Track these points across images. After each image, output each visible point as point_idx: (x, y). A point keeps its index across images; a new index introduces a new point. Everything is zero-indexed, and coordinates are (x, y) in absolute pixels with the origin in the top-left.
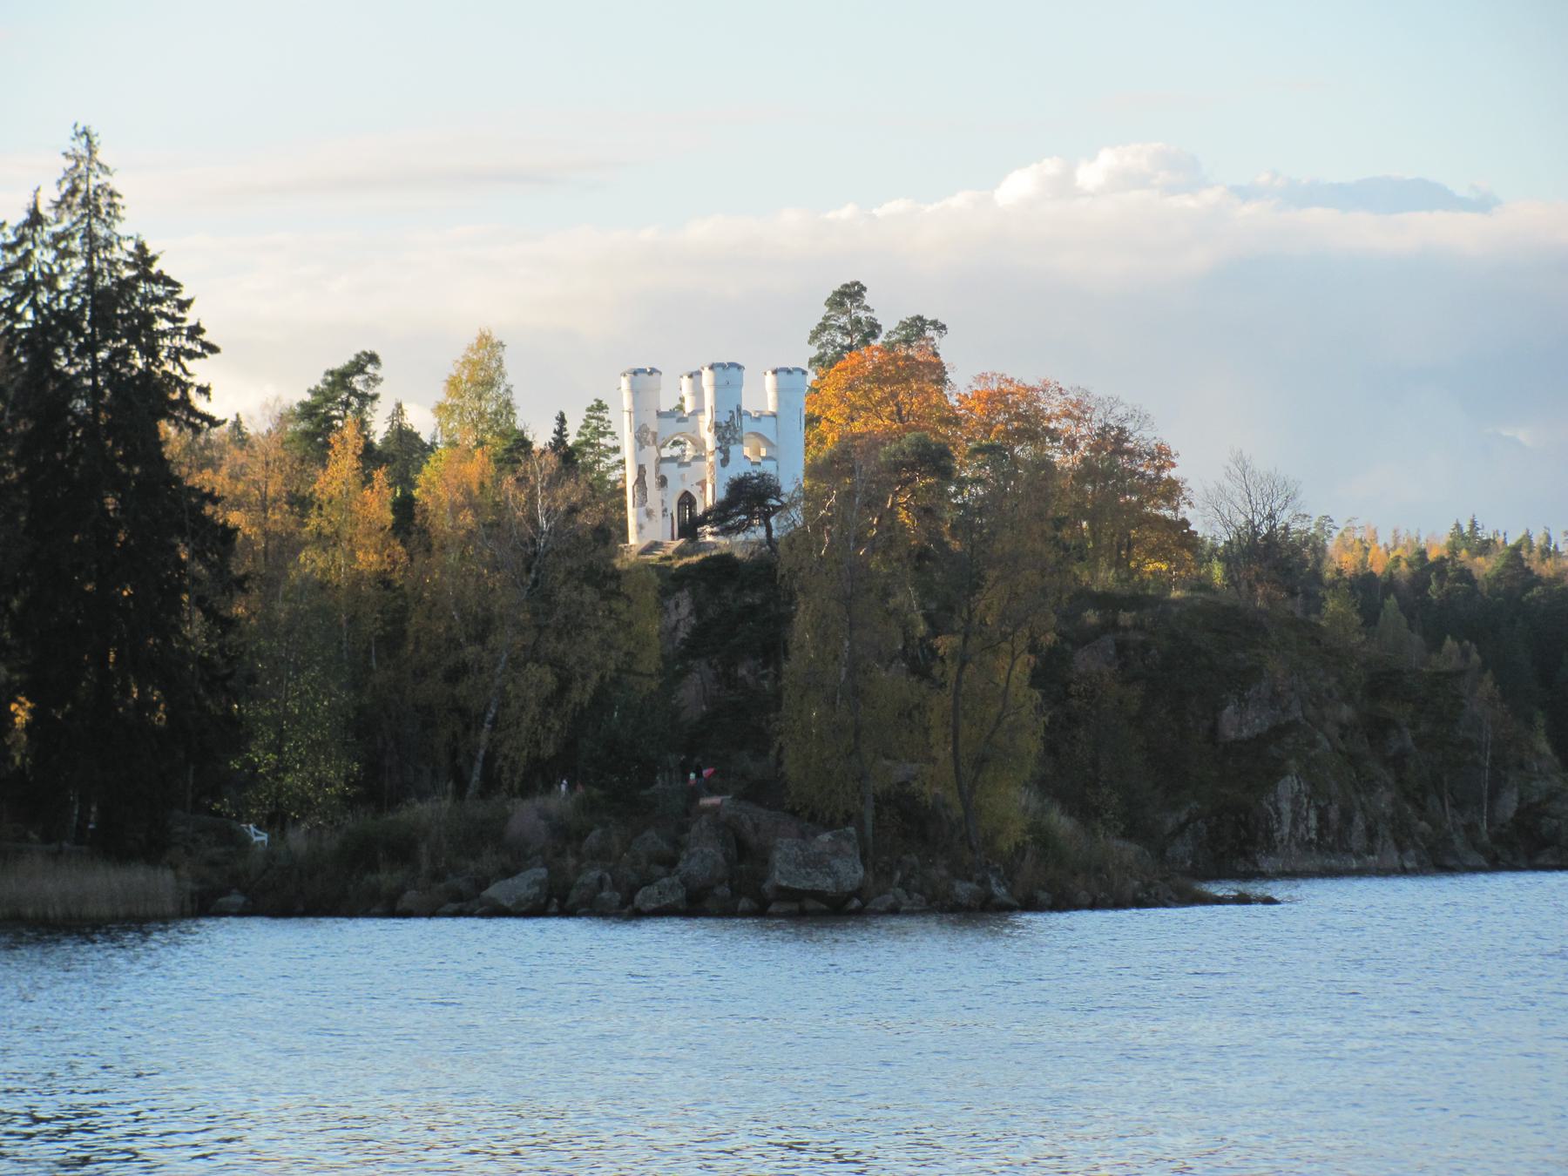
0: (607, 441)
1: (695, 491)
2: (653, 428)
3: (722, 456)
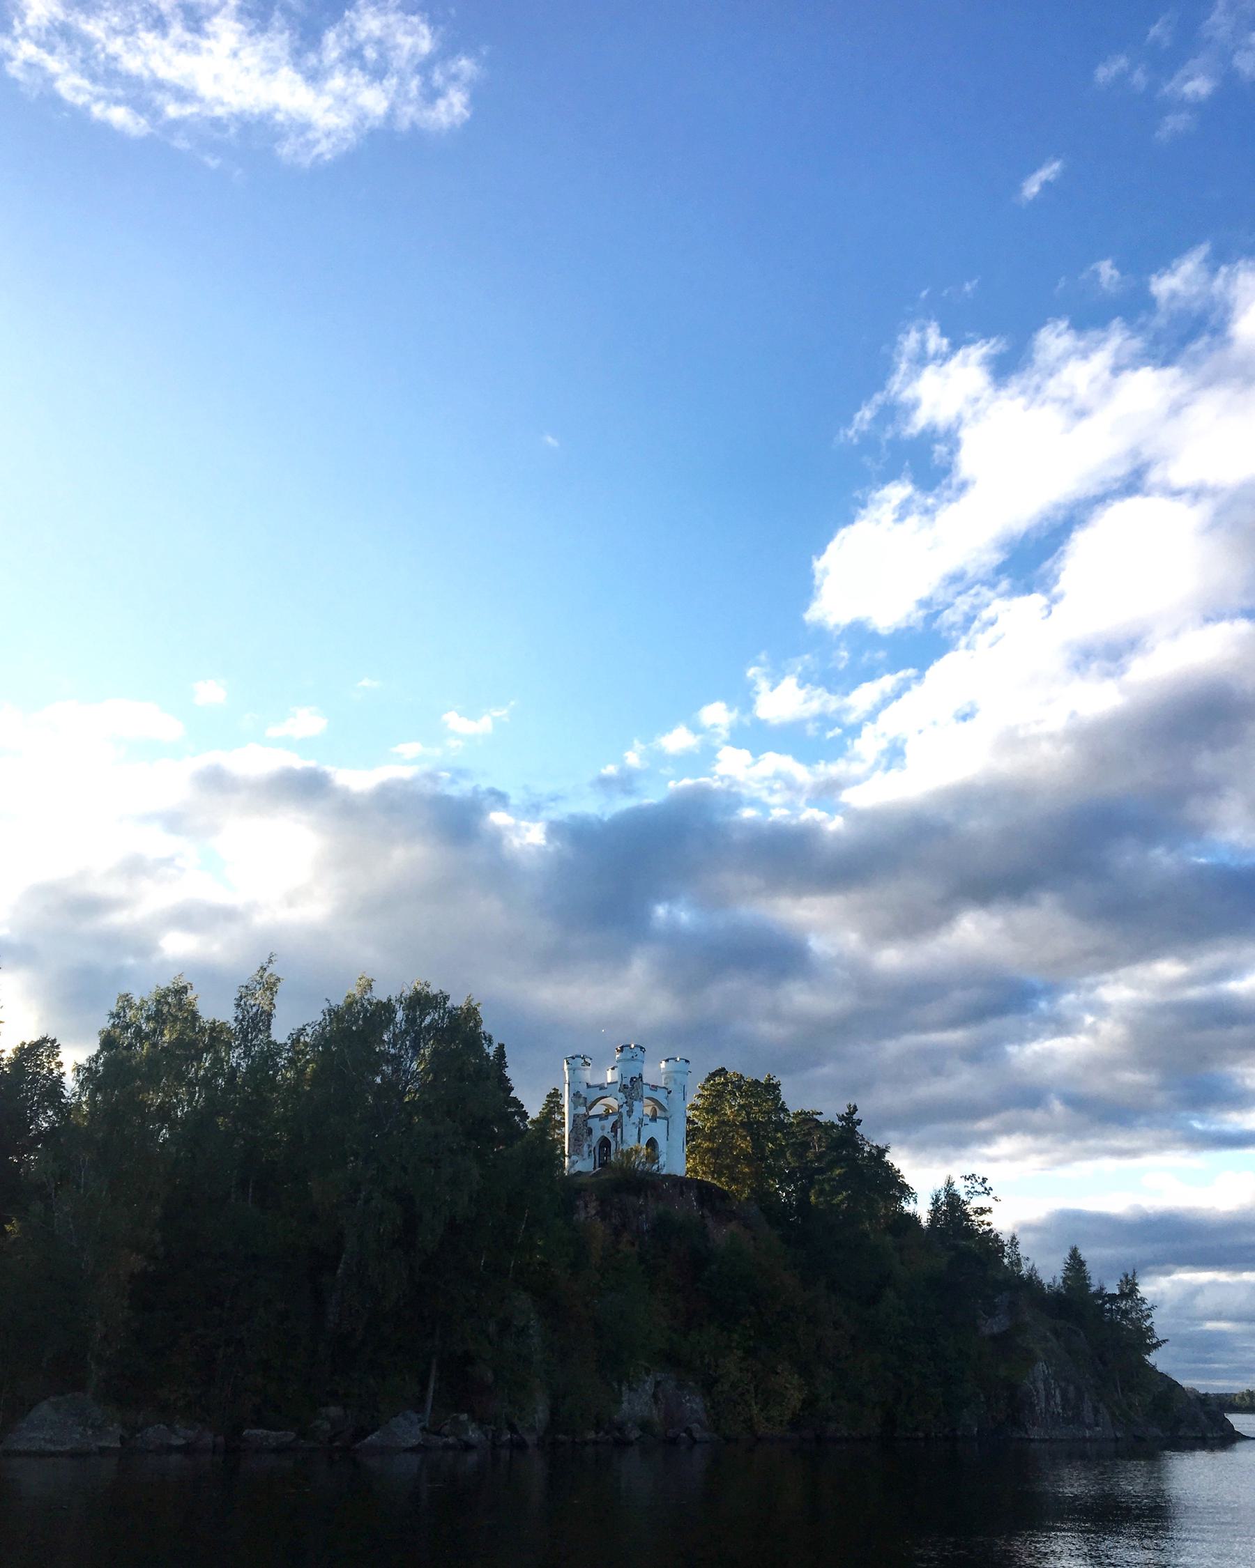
0: (558, 1117)
1: (610, 1136)
3: (628, 1108)
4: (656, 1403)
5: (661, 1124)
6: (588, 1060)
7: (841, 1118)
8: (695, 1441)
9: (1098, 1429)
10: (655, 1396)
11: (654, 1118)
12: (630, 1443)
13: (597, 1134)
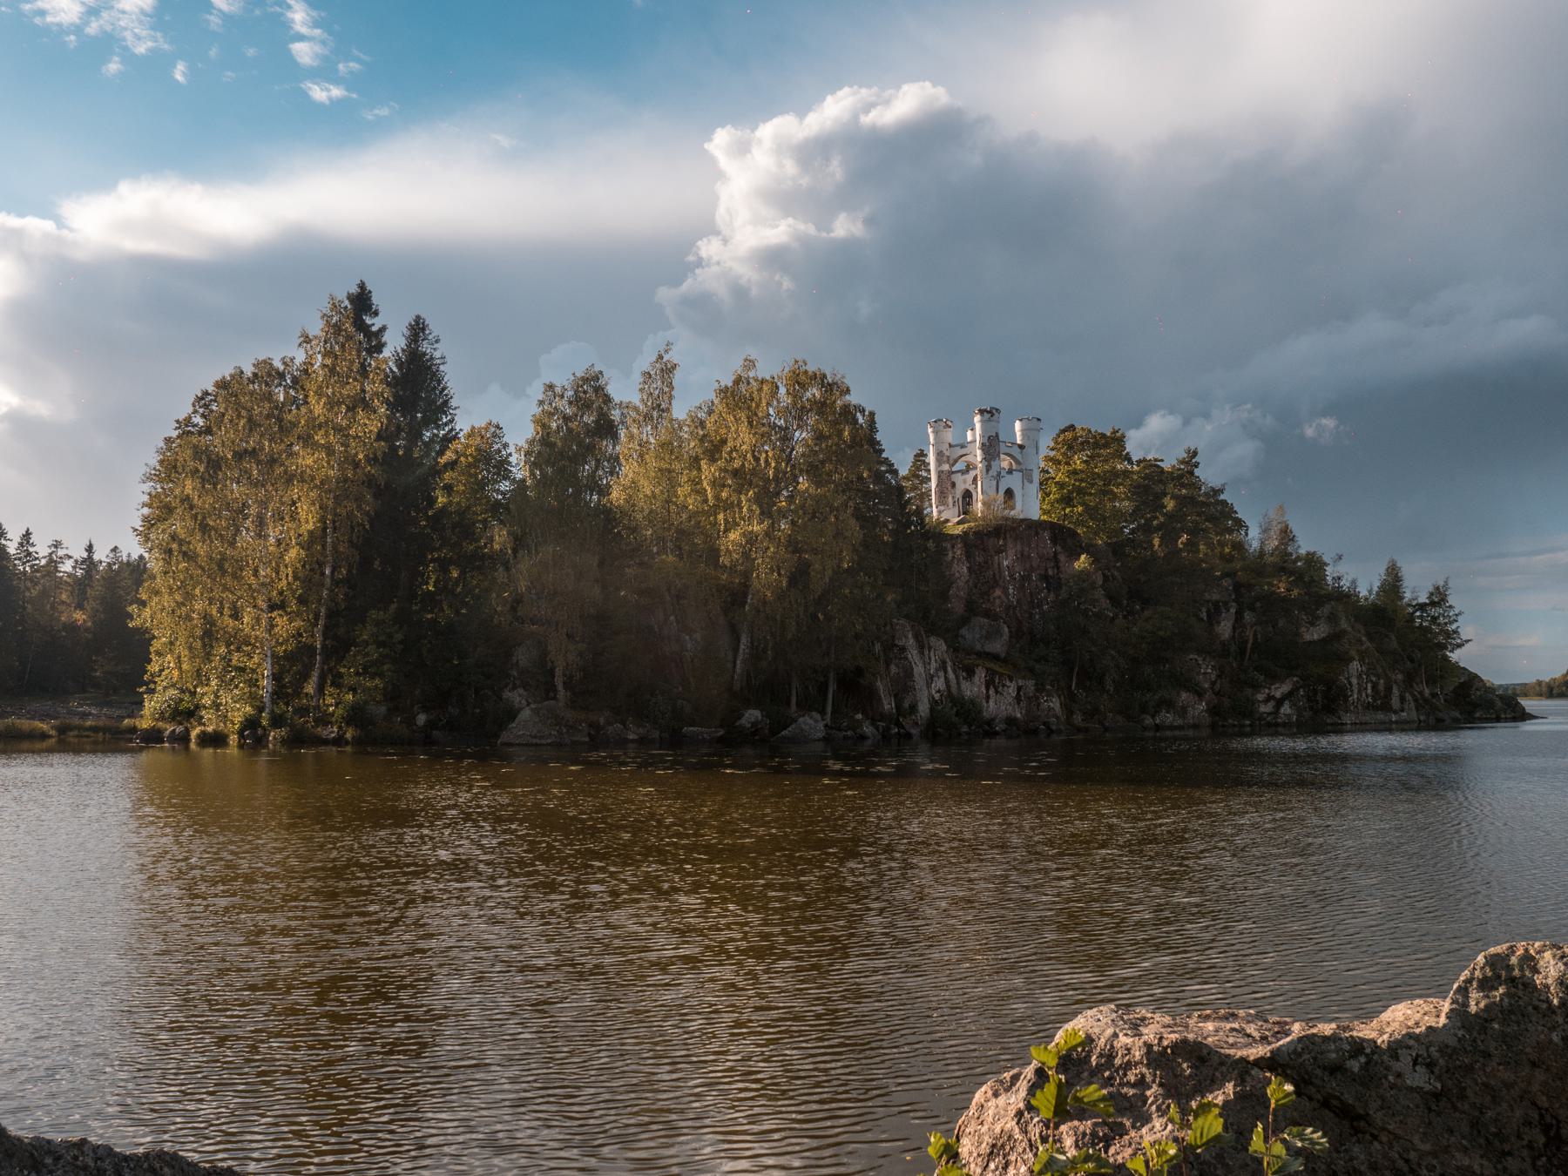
0: (924, 474)
1: (971, 488)
2: (947, 453)
4: (1018, 703)
5: (1017, 476)
6: (949, 423)
7: (1182, 462)
8: (1052, 731)
9: (1404, 714)
10: (1018, 699)
11: (1010, 472)
12: (996, 734)
13: (960, 488)
